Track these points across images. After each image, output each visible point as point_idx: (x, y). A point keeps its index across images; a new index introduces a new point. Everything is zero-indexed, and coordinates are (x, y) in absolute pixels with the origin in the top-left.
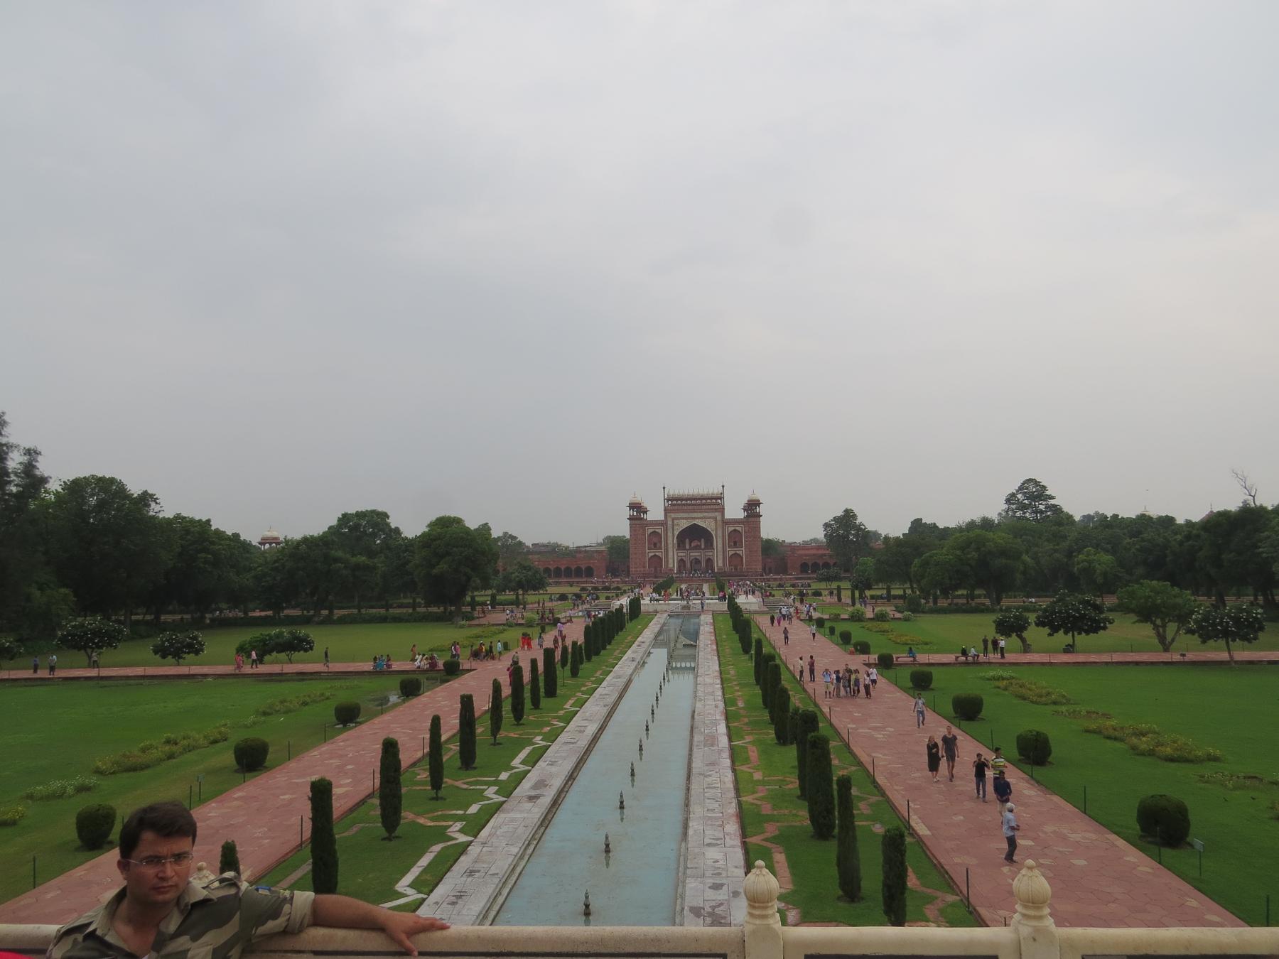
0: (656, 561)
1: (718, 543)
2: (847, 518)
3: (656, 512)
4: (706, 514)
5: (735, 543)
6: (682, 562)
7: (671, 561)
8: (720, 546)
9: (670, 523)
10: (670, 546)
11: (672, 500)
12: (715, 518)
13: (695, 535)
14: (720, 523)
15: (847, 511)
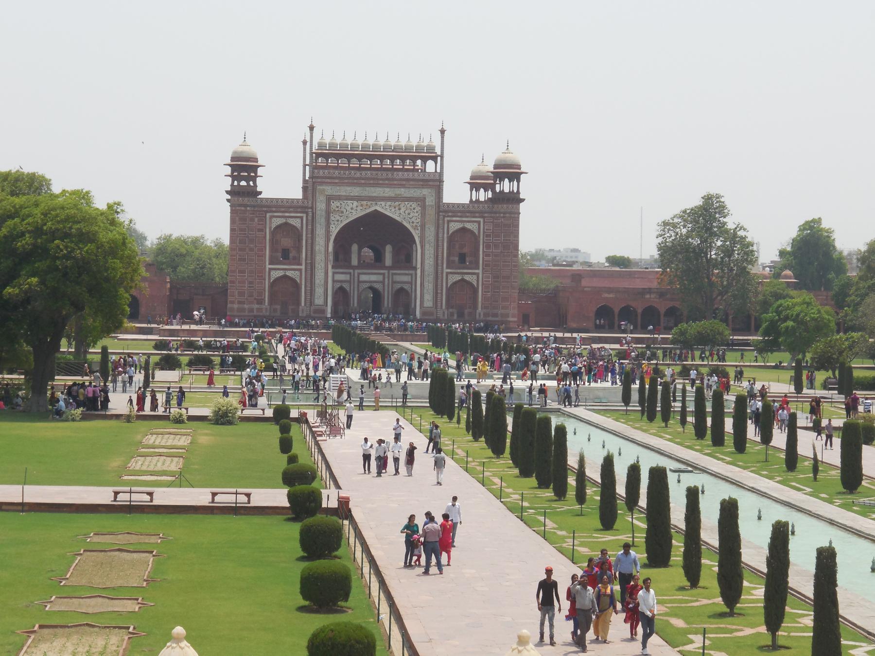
0: (286, 293)
1: (425, 256)
2: (707, 215)
3: (282, 180)
4: (402, 192)
5: (462, 258)
6: (341, 294)
7: (319, 291)
8: (429, 262)
9: (321, 206)
10: (320, 258)
11: (326, 156)
12: (422, 201)
13: (376, 237)
14: (431, 213)
15: (708, 199)
